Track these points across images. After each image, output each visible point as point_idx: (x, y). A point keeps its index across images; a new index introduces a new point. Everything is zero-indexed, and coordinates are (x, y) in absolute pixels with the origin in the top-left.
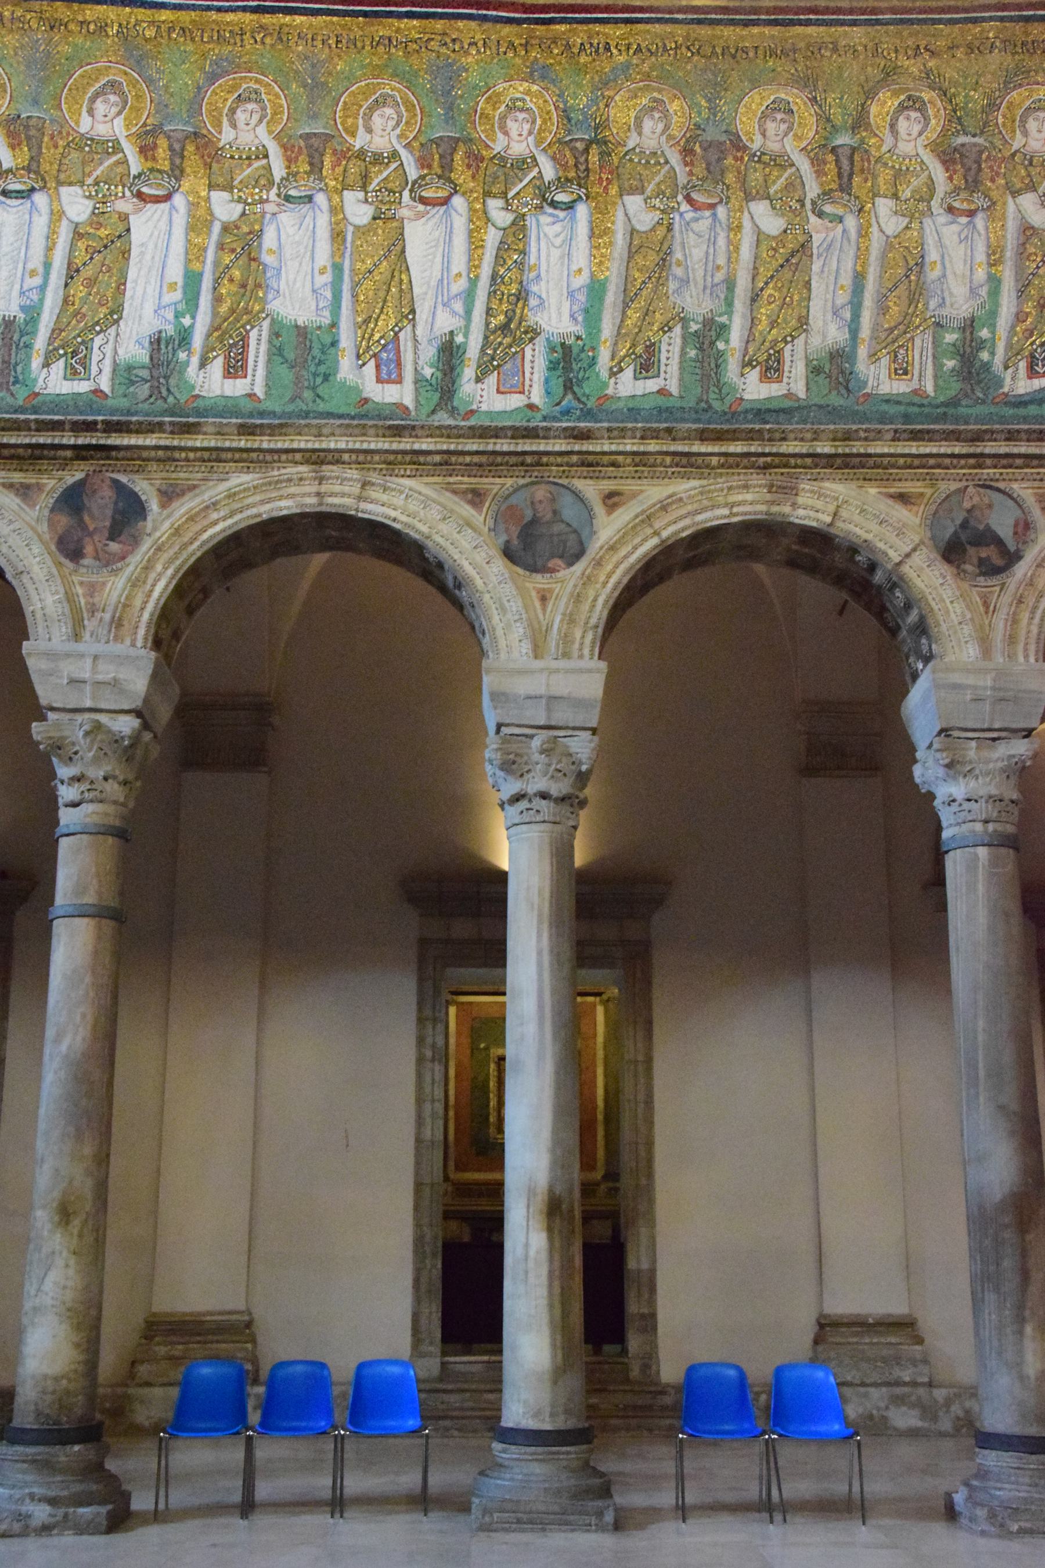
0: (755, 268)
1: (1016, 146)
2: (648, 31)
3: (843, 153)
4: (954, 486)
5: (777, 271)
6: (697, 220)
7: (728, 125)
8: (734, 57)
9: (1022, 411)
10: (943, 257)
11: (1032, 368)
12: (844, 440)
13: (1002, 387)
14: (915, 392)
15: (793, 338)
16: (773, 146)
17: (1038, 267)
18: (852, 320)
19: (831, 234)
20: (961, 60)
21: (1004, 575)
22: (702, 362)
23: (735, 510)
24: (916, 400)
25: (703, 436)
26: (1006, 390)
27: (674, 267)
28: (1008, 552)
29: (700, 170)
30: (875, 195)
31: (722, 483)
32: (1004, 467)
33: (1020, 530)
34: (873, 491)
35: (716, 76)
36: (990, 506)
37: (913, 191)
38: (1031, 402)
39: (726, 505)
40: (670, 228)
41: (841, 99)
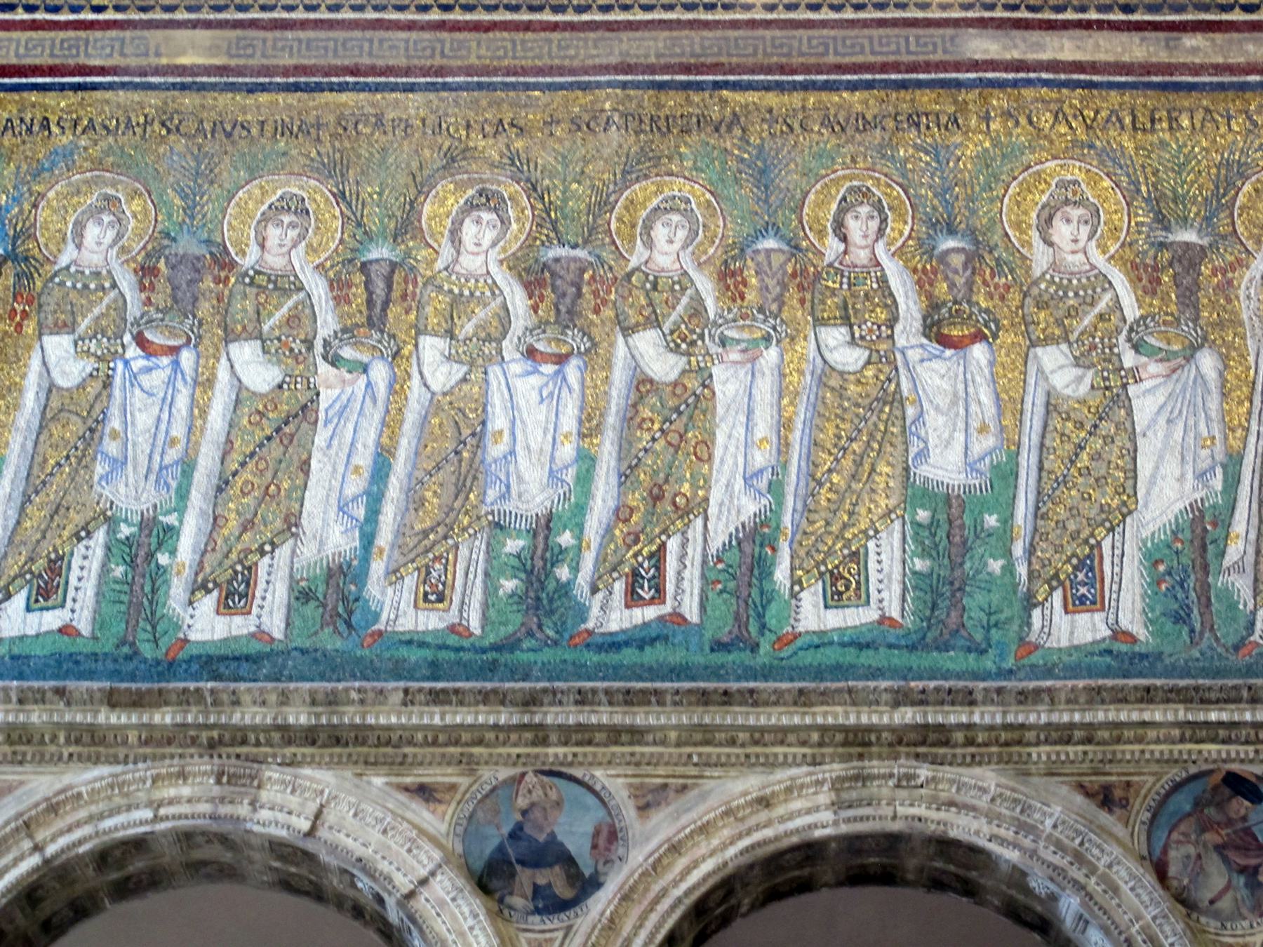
0: (229, 441)
1: (634, 262)
2: (107, 102)
3: (378, 272)
4: (504, 773)
5: (261, 445)
6: (149, 370)
7: (210, 231)
8: (229, 135)
9: (613, 658)
10: (513, 423)
11: (633, 592)
12: (330, 703)
13: (584, 620)
14: (452, 629)
15: (274, 546)
16: (275, 261)
17: (654, 440)
18: (367, 520)
19: (349, 390)
20: (560, 140)
21: (571, 913)
22: (131, 585)
23: (162, 812)
24: (453, 640)
25: (113, 700)
26: (590, 625)
27: (106, 439)
28: (579, 874)
29: (160, 299)
30: (418, 333)
31: (143, 770)
32: (578, 744)
33: (602, 842)
34: (378, 781)
35: (199, 164)
36: (558, 804)
37: (477, 327)
38: (627, 644)
39: (149, 804)
40: (107, 384)
41: (380, 194)
